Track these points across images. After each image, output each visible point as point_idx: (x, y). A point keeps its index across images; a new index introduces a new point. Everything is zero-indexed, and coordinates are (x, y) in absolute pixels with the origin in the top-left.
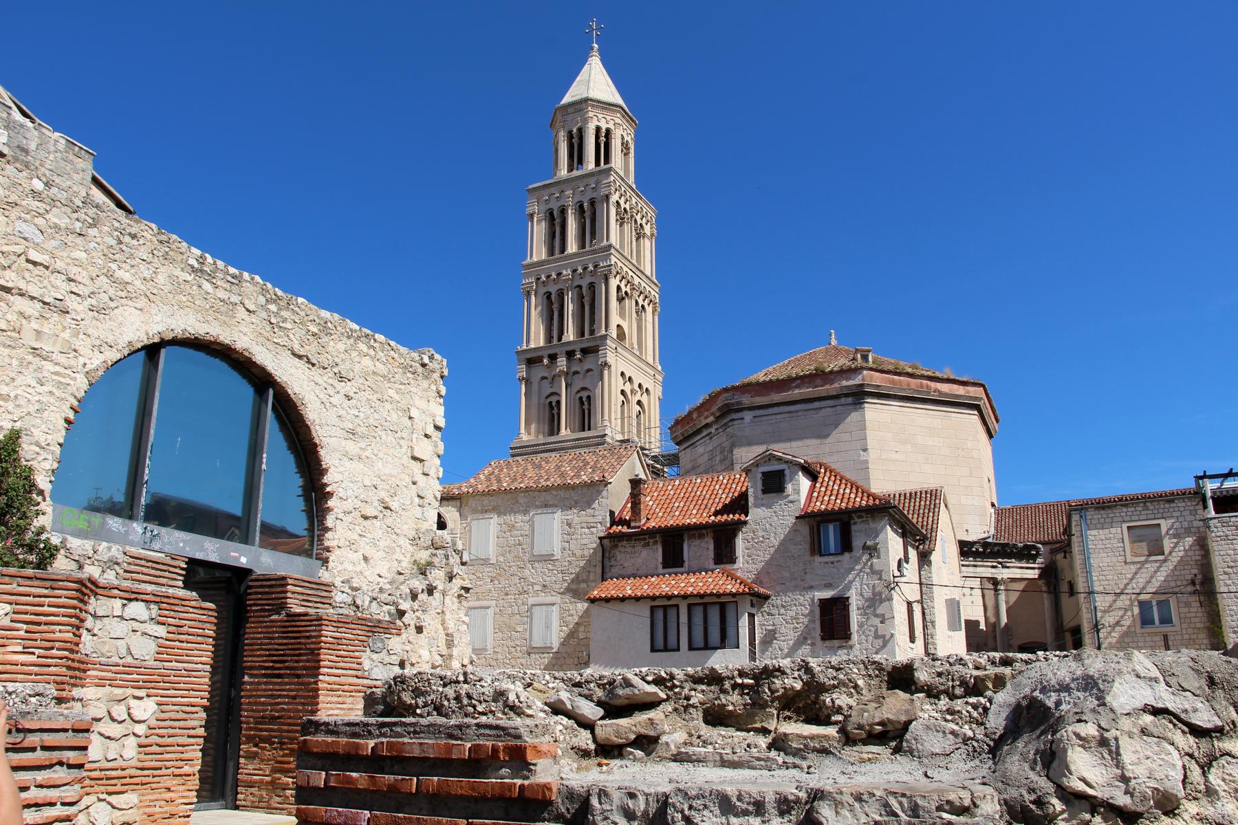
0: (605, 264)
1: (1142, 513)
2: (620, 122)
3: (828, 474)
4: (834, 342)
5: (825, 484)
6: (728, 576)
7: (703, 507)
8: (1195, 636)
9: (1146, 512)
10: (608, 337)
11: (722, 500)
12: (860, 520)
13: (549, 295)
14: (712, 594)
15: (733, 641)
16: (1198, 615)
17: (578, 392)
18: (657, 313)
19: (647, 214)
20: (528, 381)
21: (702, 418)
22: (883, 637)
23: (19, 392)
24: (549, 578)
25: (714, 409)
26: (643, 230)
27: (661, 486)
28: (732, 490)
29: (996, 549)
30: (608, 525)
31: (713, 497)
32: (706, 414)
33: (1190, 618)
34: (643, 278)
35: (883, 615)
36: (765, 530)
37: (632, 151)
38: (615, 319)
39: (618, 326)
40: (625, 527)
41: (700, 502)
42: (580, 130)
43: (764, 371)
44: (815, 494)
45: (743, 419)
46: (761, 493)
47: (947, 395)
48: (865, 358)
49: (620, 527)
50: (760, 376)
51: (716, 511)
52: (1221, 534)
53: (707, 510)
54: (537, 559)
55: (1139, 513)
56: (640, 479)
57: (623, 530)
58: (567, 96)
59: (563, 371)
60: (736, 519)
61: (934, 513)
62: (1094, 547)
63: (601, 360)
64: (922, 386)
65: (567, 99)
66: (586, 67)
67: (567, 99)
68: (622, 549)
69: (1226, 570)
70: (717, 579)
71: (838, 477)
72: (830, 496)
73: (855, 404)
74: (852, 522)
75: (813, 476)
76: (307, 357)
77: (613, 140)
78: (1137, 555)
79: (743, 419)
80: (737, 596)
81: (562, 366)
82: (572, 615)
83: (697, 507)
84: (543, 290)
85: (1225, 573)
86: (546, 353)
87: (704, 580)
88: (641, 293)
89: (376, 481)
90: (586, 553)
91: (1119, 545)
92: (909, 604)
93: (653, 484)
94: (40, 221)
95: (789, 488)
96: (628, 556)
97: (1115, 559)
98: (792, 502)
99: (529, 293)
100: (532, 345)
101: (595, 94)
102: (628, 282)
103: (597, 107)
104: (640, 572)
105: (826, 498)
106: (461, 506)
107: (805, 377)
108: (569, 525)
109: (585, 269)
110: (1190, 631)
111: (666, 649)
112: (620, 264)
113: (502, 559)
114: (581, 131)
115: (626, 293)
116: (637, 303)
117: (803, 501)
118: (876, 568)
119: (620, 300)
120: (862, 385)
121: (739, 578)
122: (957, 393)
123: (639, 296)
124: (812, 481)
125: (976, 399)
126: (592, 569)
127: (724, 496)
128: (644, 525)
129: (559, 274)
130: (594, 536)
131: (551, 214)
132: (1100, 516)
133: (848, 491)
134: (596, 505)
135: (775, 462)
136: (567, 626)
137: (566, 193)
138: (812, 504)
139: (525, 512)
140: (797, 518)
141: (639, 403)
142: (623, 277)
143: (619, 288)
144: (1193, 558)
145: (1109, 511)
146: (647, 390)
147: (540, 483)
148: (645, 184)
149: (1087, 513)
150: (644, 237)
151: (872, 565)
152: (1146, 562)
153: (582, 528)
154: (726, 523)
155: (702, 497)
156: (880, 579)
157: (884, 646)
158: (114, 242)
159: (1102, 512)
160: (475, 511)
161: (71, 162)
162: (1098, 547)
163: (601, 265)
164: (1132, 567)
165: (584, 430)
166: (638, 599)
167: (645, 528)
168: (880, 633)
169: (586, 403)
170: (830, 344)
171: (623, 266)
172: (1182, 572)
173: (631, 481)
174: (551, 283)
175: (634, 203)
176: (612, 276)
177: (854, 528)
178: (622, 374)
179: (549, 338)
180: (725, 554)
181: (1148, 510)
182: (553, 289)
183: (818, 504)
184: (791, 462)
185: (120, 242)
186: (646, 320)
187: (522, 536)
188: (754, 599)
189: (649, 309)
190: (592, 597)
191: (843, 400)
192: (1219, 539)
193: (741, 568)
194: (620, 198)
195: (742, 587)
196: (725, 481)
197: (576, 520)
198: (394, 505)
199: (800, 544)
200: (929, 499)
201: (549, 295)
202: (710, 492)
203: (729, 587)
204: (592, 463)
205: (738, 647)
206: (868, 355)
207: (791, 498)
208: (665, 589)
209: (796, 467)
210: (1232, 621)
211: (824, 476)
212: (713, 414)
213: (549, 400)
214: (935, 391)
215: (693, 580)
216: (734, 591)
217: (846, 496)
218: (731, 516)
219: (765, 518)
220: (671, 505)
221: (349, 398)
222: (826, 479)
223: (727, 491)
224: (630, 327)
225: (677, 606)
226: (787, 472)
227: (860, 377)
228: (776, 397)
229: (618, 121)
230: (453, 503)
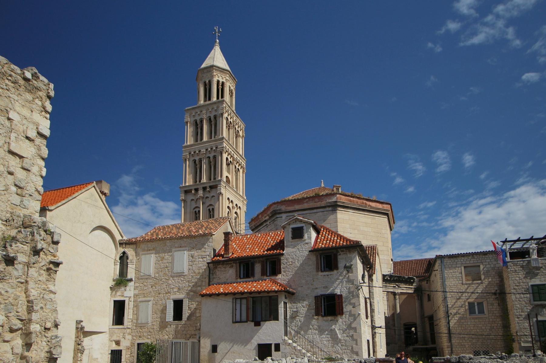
0: (221, 147)
1: (472, 260)
2: (229, 79)
3: (325, 231)
4: (323, 185)
5: (324, 235)
6: (273, 282)
7: (261, 247)
8: (495, 320)
9: (473, 260)
10: (222, 181)
11: (271, 244)
12: (343, 253)
13: (195, 161)
14: (264, 292)
16: (497, 309)
18: (244, 173)
19: (240, 126)
21: (263, 217)
22: (354, 315)
24: (182, 285)
25: (269, 212)
26: (239, 133)
27: (240, 238)
28: (276, 239)
30: (212, 257)
31: (267, 242)
32: (265, 215)
33: (493, 311)
34: (239, 155)
35: (354, 303)
36: (293, 258)
37: (234, 94)
38: (225, 174)
39: (227, 177)
40: (221, 257)
41: (260, 245)
43: (292, 196)
44: (319, 240)
46: (291, 239)
47: (374, 208)
48: (338, 189)
49: (218, 258)
50: (290, 198)
51: (268, 249)
52: (513, 269)
53: (263, 249)
54: (175, 275)
55: (469, 260)
56: (229, 232)
57: (220, 259)
59: (201, 196)
60: (278, 252)
61: (373, 257)
62: (447, 276)
63: (218, 191)
64: (363, 203)
66: (213, 51)
67: (203, 66)
68: (219, 269)
69: (515, 287)
70: (268, 284)
71: (330, 232)
72: (327, 241)
74: (338, 254)
75: (318, 231)
77: (225, 88)
78: (467, 280)
80: (278, 293)
81: (201, 194)
82: (193, 304)
83: (258, 247)
84: (192, 159)
85: (514, 289)
87: (261, 284)
88: (237, 162)
90: (201, 271)
91: (460, 275)
92: (365, 298)
93: (236, 237)
95: (306, 236)
97: (457, 282)
98: (307, 244)
99: (186, 160)
100: (187, 184)
102: (232, 156)
103: (218, 70)
104: (228, 281)
105: (325, 242)
106: (136, 248)
107: (310, 197)
108: (192, 257)
109: (212, 149)
110: (493, 317)
112: (228, 147)
113: (157, 275)
114: (210, 82)
115: (230, 161)
117: (313, 243)
118: (351, 278)
119: (228, 165)
120: (336, 202)
121: (279, 283)
122: (378, 207)
123: (236, 164)
124: (317, 234)
125: (387, 210)
126: (204, 280)
127: (272, 242)
128: (230, 256)
129: (200, 151)
130: (205, 262)
132: (450, 261)
133: (336, 238)
134: (206, 246)
135: (299, 223)
136: (190, 310)
137: (203, 112)
138: (317, 245)
139: (170, 251)
140: (310, 251)
142: (229, 154)
143: (227, 159)
144: (496, 282)
145: (455, 259)
147: (178, 235)
148: (240, 111)
149: (445, 260)
150: (239, 137)
151: (348, 276)
152: (472, 284)
153: (199, 258)
154: (272, 255)
155: (261, 243)
156: (353, 284)
157: (355, 320)
159: (452, 259)
160: (144, 250)
162: (449, 276)
163: (219, 147)
164: (466, 286)
166: (226, 294)
167: (231, 258)
168: (353, 313)
170: (321, 186)
171: (229, 148)
172: (490, 289)
173: (224, 233)
175: (235, 119)
176: (224, 152)
177: (339, 257)
179: (195, 181)
181: (474, 258)
182: (197, 158)
183: (320, 245)
184: (307, 223)
186: (239, 176)
187: (168, 263)
188: (287, 294)
189: (241, 171)
190: (202, 293)
192: (512, 272)
193: (280, 278)
194: (228, 116)
195: (281, 287)
196: (273, 235)
197: (196, 254)
199: (311, 266)
200: (370, 250)
202: (265, 240)
203: (274, 287)
204: (205, 226)
206: (339, 189)
208: (241, 289)
209: (309, 225)
210: (517, 312)
212: (268, 215)
214: (369, 206)
215: (255, 284)
216: (276, 289)
217: (335, 241)
218: (275, 251)
219: (293, 252)
220: (245, 247)
222: (324, 233)
223: (273, 239)
224: (232, 177)
226: (305, 228)
227: (336, 198)
228: (297, 207)
229: (228, 78)
230: (131, 246)
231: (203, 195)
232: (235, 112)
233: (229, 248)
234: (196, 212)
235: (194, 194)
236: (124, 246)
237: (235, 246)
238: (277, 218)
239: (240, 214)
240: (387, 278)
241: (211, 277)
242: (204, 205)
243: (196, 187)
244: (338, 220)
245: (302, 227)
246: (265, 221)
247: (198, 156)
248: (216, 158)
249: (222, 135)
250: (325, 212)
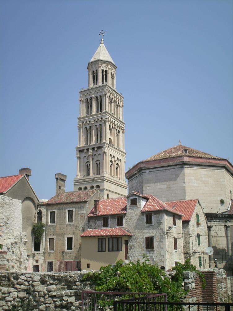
13: (86, 128)
14: (114, 235)
15: (120, 249)
20: (79, 158)
26: (119, 104)
29: (226, 216)
38: (108, 136)
42: (97, 71)
44: (146, 205)
45: (146, 172)
58: (93, 58)
59: (91, 155)
63: (103, 151)
65: (92, 60)
73: (181, 168)
79: (146, 172)
86: (85, 148)
89: (3, 217)
100: (81, 146)
101: (102, 58)
111: (102, 251)
112: (110, 118)
115: (112, 127)
116: (116, 130)
118: (161, 228)
119: (110, 130)
123: (117, 128)
129: (90, 121)
131: (87, 100)
141: (117, 164)
143: (110, 126)
146: (120, 159)
150: (119, 107)
163: (103, 118)
165: (98, 174)
166: (94, 236)
169: (99, 165)
174: (87, 124)
178: (111, 155)
180: (120, 223)
182: (88, 127)
186: (120, 136)
191: (178, 166)
201: (86, 128)
203: (119, 233)
205: (121, 251)
206: (187, 151)
207: (138, 207)
208: (102, 233)
211: (150, 200)
212: (137, 170)
213: (87, 164)
225: (105, 238)
226: (137, 199)
231: (92, 153)
232: (115, 90)
233: (97, 209)
235: (86, 153)
236: (40, 206)
237: (101, 207)
238: (143, 173)
239: (121, 165)
240: (219, 216)
242: (93, 161)
243: (87, 148)
244: (185, 174)
245: (136, 199)
246: (136, 174)
247: (89, 125)
249: (105, 110)
250: (176, 169)
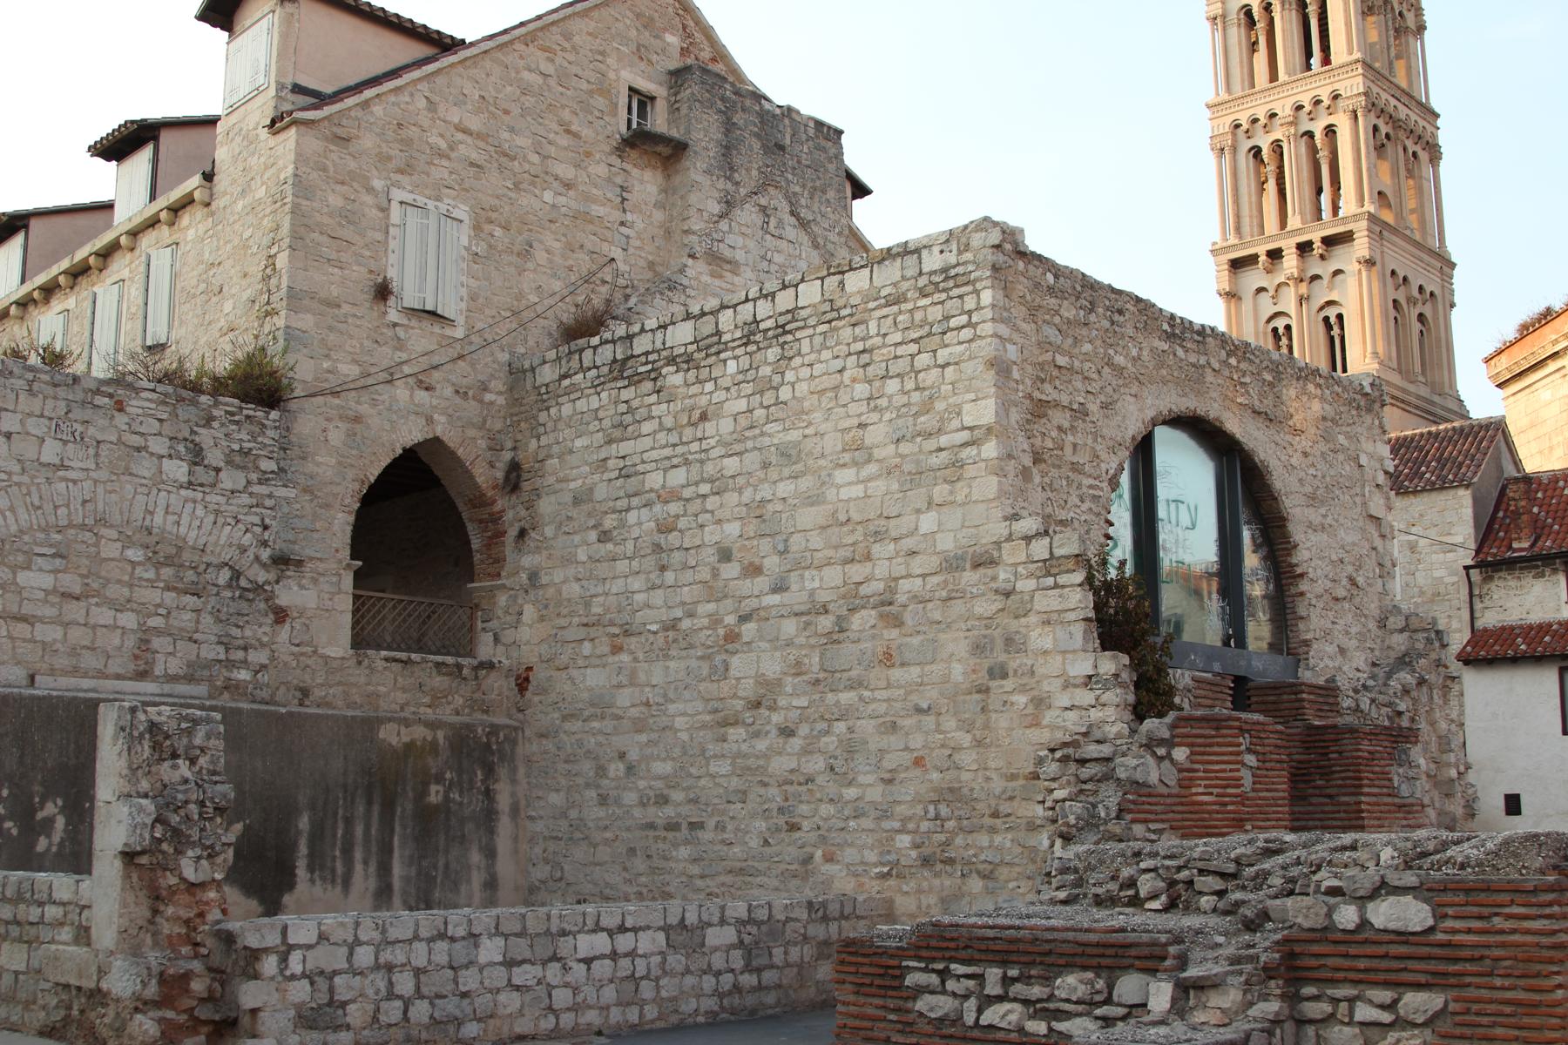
17: (1321, 309)
23: (1072, 514)
68: (1501, 583)
76: (1266, 414)
86: (1261, 250)
94: (1057, 320)
96: (1512, 593)
116: (1405, 149)
141: (1421, 318)
146: (1432, 294)
158: (1106, 324)
161: (824, 150)
178: (1393, 273)
185: (1113, 323)
198: (1360, 580)
201: (1257, 152)
213: (1272, 325)
221: (1305, 454)
234: (1275, 330)
241: (1478, 606)
248: (1335, 132)
